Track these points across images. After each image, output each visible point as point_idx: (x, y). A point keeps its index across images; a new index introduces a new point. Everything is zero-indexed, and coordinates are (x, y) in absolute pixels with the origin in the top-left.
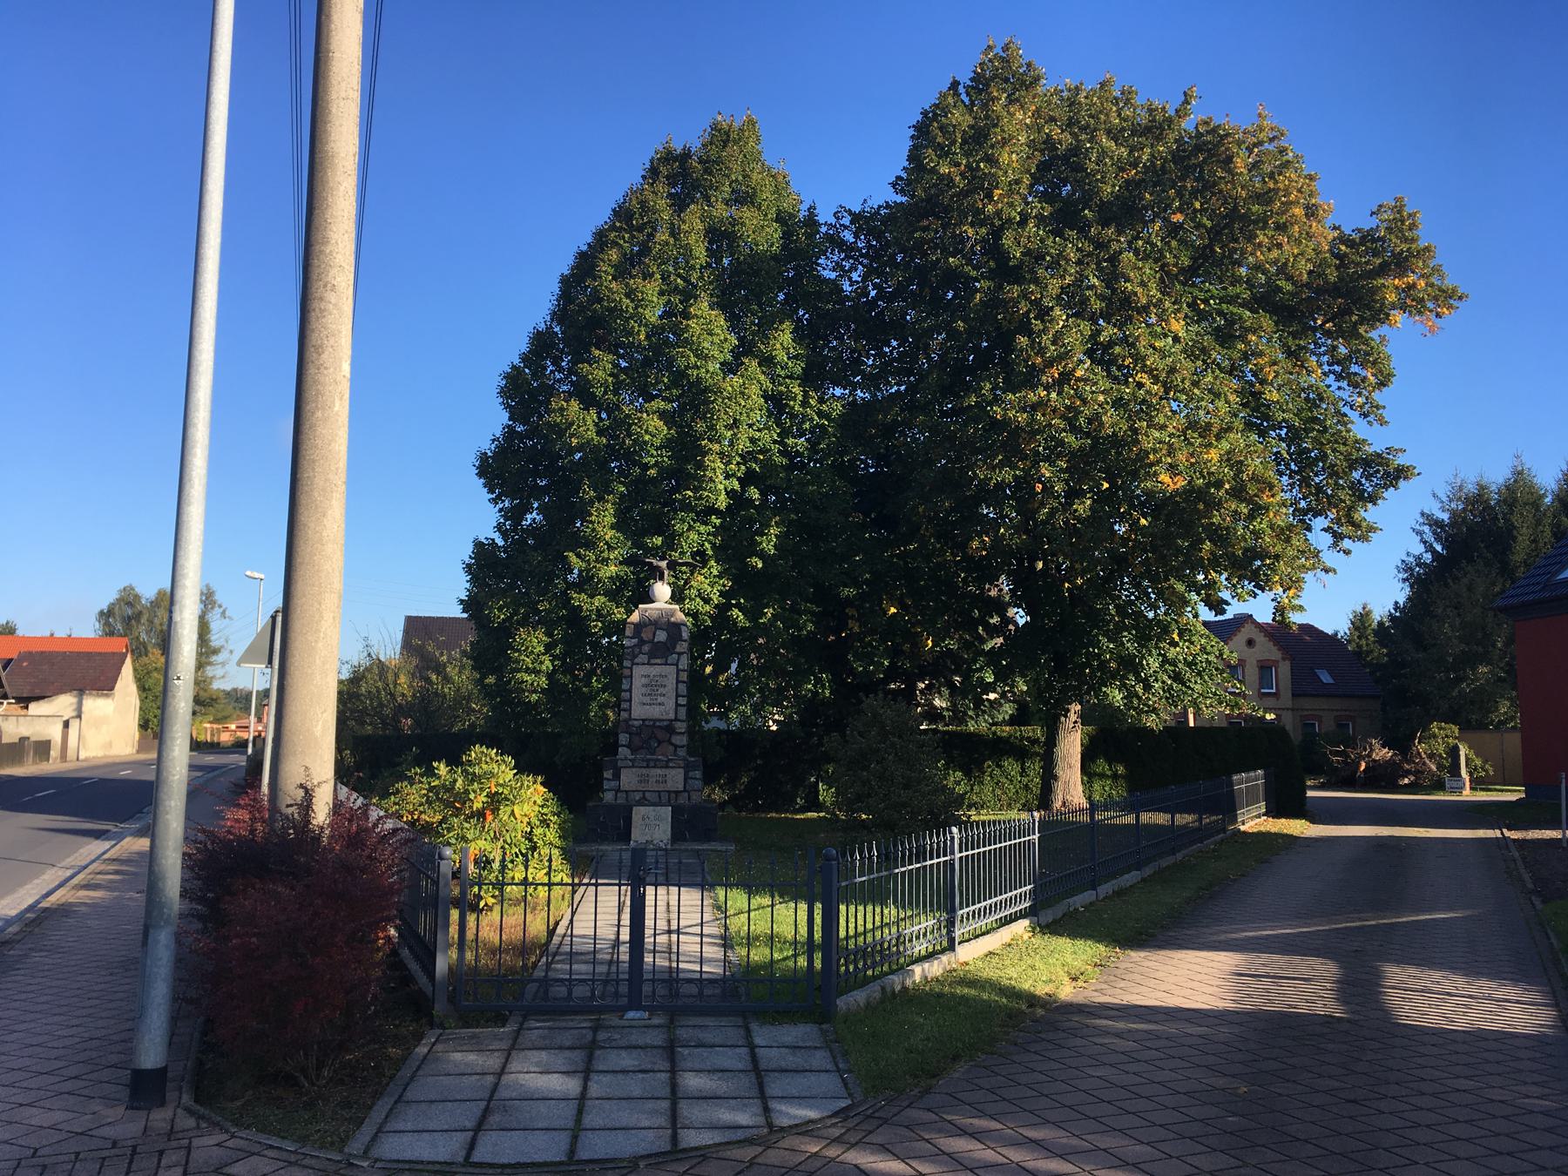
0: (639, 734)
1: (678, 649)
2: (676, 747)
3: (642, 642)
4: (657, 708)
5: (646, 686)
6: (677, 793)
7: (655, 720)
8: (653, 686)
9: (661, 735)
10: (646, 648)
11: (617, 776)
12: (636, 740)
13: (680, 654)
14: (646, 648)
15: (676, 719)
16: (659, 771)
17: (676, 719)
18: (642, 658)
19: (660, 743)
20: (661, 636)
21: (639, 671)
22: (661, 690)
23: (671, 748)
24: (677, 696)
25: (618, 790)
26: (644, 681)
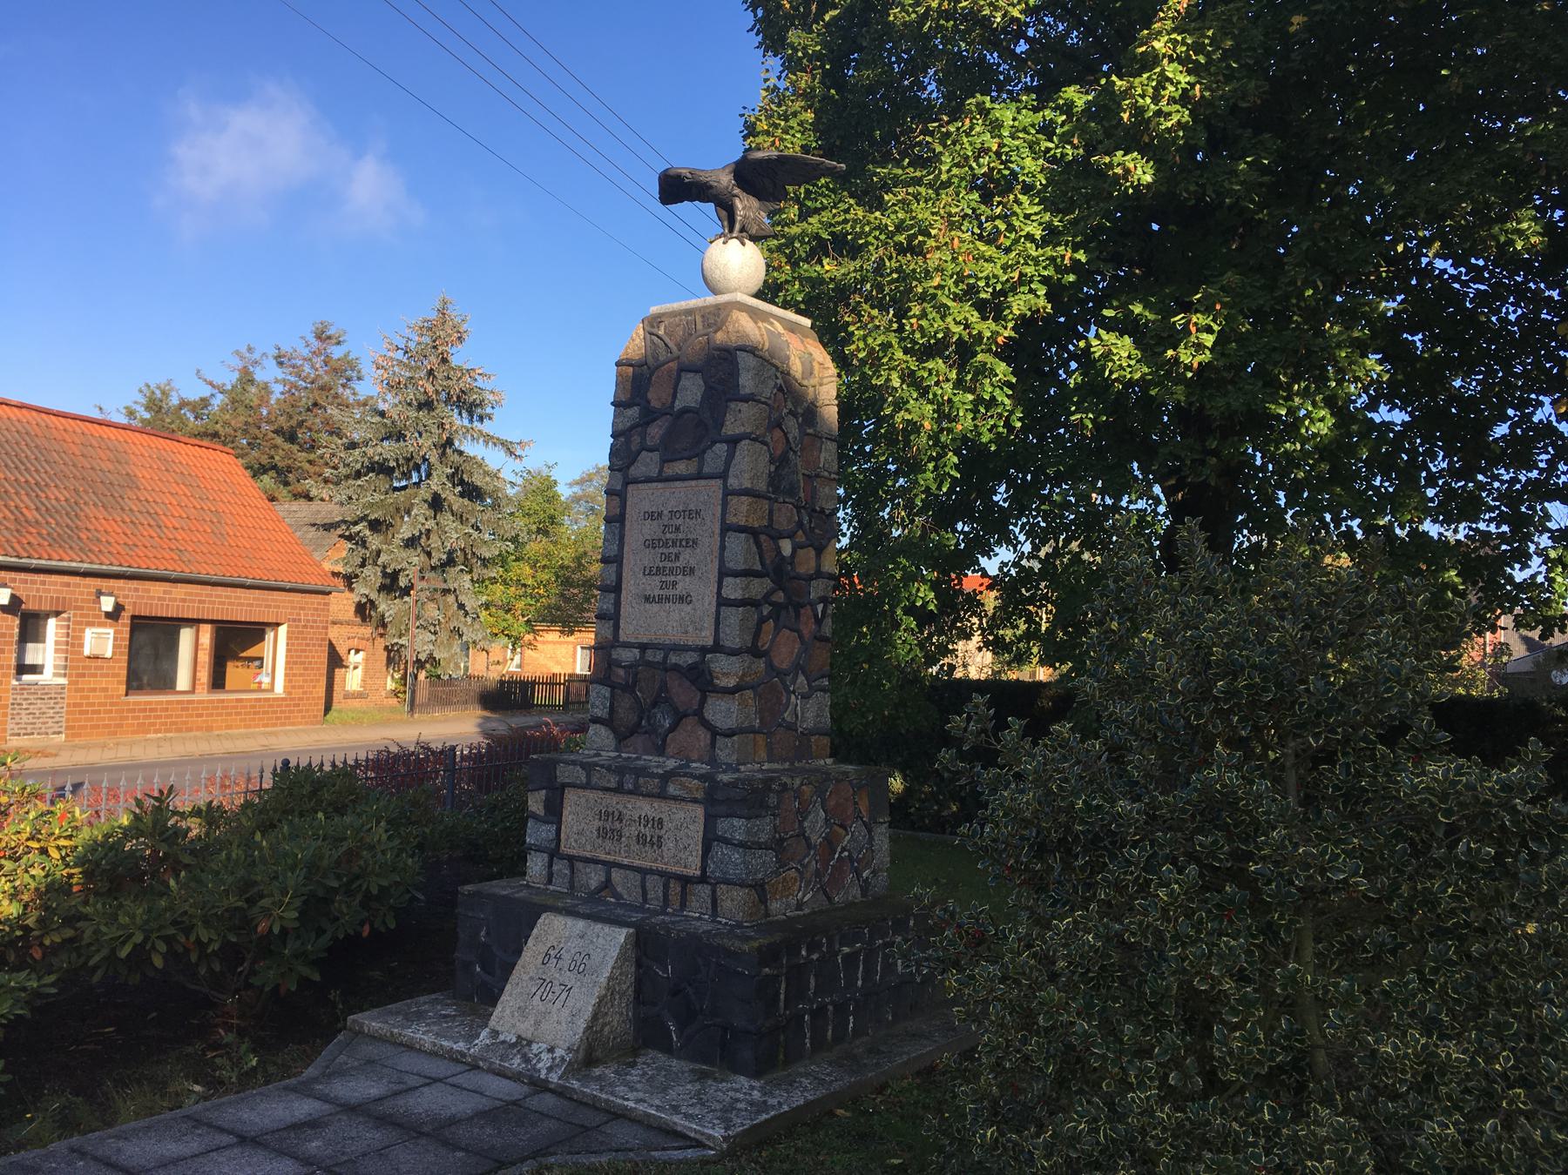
0: (629, 688)
1: (731, 427)
2: (715, 733)
4: (678, 612)
5: (651, 544)
6: (685, 880)
9: (683, 694)
10: (656, 431)
11: (554, 811)
13: (733, 441)
14: (656, 431)
15: (717, 647)
16: (646, 808)
17: (717, 647)
19: (679, 718)
20: (691, 392)
22: (687, 557)
23: (703, 736)
24: (723, 573)
25: (554, 853)
26: (651, 529)
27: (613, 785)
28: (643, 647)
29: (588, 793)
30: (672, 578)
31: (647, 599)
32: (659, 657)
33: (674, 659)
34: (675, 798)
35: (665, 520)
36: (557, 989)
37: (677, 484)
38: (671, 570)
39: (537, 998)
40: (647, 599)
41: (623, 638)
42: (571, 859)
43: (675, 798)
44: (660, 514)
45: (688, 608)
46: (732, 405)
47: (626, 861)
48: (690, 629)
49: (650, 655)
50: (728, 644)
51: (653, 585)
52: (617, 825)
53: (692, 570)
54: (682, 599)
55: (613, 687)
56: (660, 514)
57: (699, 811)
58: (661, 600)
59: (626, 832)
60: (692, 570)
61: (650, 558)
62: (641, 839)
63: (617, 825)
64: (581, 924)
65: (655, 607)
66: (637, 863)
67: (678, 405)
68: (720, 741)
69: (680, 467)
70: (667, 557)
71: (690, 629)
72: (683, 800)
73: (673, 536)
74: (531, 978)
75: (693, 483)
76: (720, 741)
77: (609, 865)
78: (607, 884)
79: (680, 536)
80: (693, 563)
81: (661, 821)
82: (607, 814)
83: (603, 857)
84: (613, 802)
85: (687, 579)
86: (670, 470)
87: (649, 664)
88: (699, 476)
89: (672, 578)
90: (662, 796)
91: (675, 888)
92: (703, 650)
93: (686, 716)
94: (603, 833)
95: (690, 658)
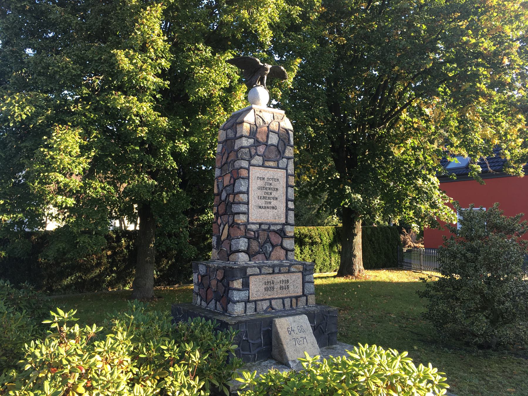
0: (256, 238)
3: (257, 143)
4: (272, 212)
5: (260, 188)
6: (297, 298)
7: (270, 224)
8: (268, 189)
11: (246, 285)
12: (255, 246)
13: (288, 158)
14: (261, 149)
15: (287, 223)
16: (282, 277)
17: (287, 223)
18: (257, 160)
19: (273, 246)
20: (274, 140)
21: (256, 172)
22: (274, 194)
23: (283, 252)
24: (287, 200)
25: (248, 301)
26: (260, 183)
27: (271, 272)
28: (260, 224)
29: (259, 276)
30: (269, 201)
31: (260, 207)
32: (266, 227)
33: (272, 228)
34: (294, 272)
35: (266, 180)
36: (301, 339)
37: (269, 169)
38: (269, 198)
39: (297, 345)
40: (260, 207)
41: (250, 221)
42: (255, 301)
43: (294, 272)
44: (264, 179)
45: (276, 211)
46: (288, 147)
47: (276, 297)
48: (277, 218)
49: (263, 227)
50: (291, 222)
51: (262, 203)
52: (272, 285)
53: (277, 199)
54: (273, 208)
55: (249, 239)
56: (264, 179)
57: (300, 275)
58: (265, 208)
59: (275, 287)
60: (277, 199)
61: (261, 193)
62: (282, 288)
63: (272, 285)
64: (291, 318)
65: (263, 210)
66: (281, 296)
67: (269, 143)
68: (289, 253)
69: (271, 164)
70: (267, 193)
71: (277, 218)
72: (296, 272)
73: (269, 186)
74: (290, 340)
75: (276, 170)
76: (289, 253)
77: (270, 300)
78: (271, 306)
79: (272, 187)
80: (276, 196)
81: (288, 281)
82: (268, 282)
83: (268, 297)
84: (269, 278)
85: (275, 201)
86: (267, 164)
87: (264, 230)
88: (278, 168)
89: (269, 201)
90: (289, 272)
91: (294, 300)
92: (283, 225)
93: (277, 245)
94: (266, 289)
95: (279, 227)
